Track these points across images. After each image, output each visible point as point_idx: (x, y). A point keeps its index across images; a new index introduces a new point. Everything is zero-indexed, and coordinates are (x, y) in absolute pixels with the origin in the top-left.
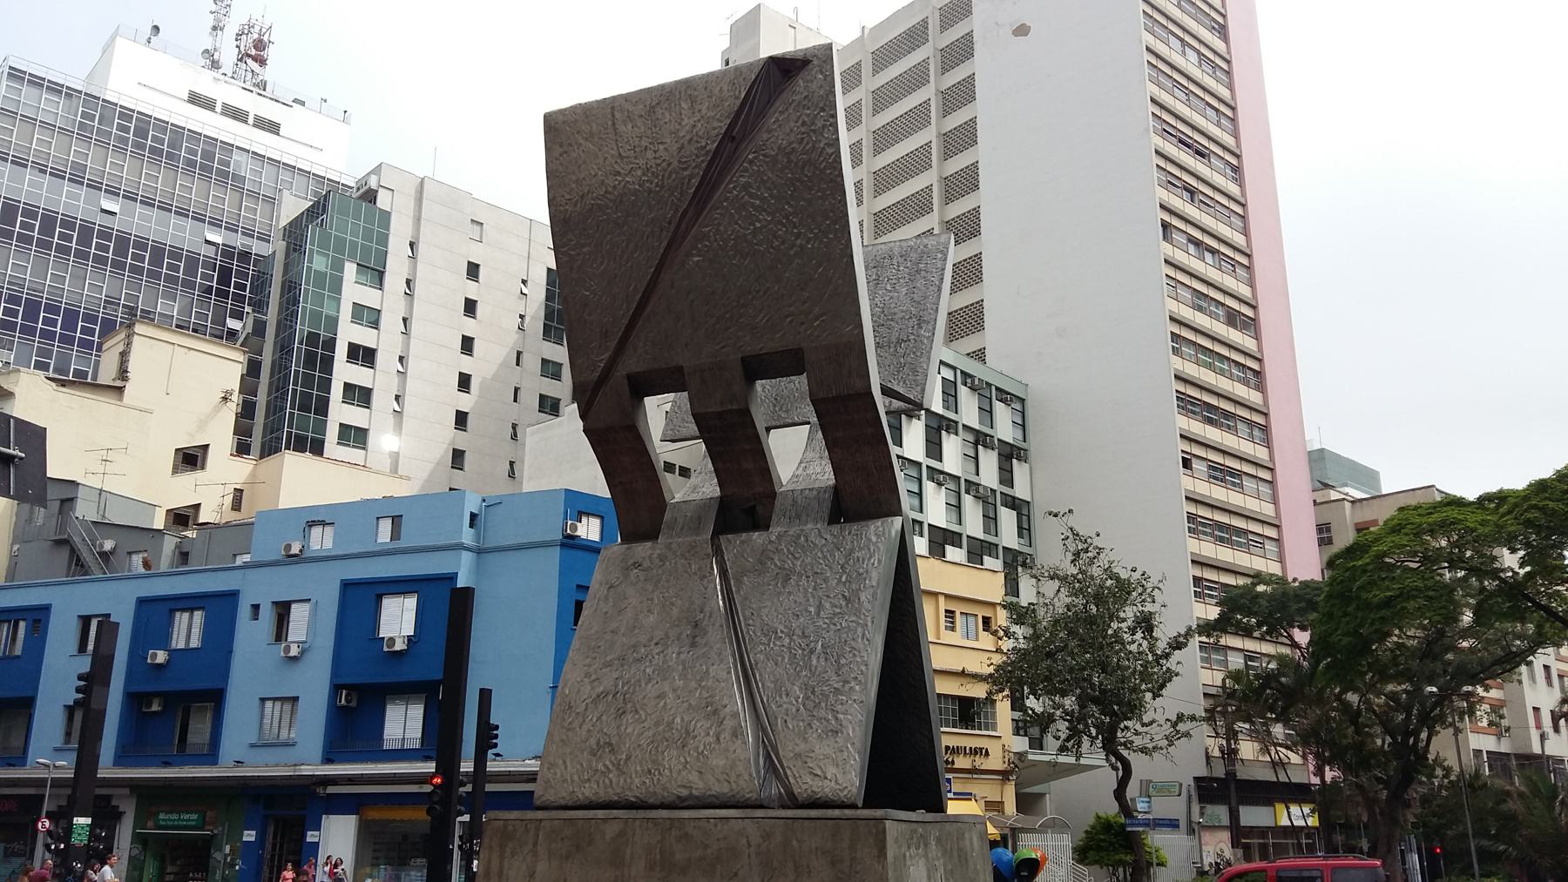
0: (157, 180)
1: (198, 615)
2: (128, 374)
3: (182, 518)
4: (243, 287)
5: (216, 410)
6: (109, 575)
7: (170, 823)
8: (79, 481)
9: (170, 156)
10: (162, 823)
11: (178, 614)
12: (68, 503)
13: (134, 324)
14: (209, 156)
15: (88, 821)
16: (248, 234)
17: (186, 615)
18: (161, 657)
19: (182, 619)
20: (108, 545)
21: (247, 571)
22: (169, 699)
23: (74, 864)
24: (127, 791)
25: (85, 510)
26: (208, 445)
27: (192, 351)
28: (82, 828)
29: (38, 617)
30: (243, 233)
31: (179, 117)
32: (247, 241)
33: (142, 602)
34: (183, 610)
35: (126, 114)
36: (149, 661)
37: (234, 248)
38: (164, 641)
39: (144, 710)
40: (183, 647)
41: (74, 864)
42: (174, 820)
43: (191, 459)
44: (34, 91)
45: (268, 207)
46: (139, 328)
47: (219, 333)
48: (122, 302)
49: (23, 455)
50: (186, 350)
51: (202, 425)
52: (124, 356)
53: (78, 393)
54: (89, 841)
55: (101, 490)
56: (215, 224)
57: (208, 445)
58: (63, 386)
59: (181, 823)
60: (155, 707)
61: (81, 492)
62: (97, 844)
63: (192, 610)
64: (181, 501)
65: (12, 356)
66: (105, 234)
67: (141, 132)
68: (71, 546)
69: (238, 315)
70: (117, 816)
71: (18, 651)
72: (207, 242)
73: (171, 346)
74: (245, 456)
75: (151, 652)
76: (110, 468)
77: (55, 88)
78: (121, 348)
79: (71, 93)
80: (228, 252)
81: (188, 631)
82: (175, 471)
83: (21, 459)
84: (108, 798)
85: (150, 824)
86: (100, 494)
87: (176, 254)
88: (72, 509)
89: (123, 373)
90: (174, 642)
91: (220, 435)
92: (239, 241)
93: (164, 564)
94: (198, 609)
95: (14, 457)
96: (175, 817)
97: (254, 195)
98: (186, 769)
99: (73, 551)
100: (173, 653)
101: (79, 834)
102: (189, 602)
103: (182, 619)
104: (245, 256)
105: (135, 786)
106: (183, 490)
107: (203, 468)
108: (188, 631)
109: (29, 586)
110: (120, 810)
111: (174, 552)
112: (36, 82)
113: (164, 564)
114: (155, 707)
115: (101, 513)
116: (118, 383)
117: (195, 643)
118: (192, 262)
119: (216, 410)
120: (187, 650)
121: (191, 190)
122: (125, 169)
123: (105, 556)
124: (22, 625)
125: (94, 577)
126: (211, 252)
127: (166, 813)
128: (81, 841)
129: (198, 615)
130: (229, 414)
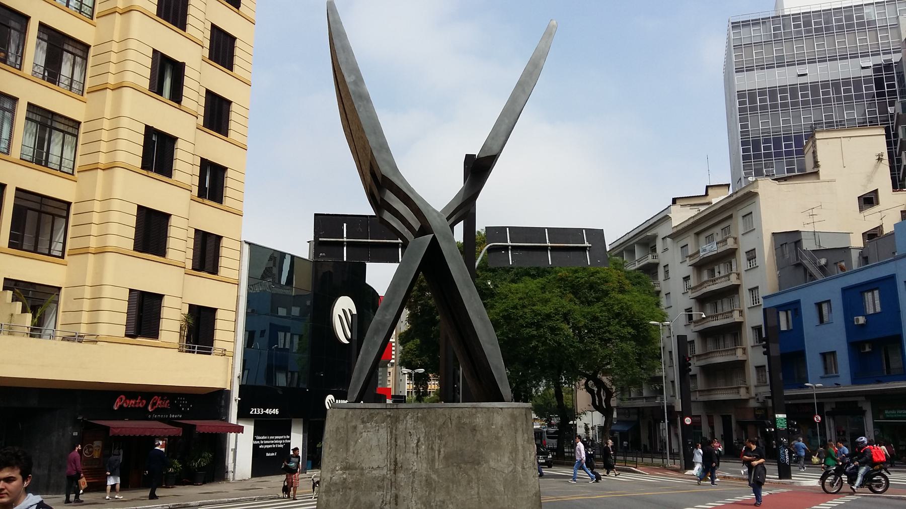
0: (822, 46)
1: (876, 293)
2: (819, 163)
3: (871, 236)
4: (893, 86)
5: (876, 167)
6: (825, 278)
7: (892, 416)
8: (800, 230)
9: (827, 29)
10: (888, 416)
11: (866, 294)
12: (798, 243)
13: (811, 137)
14: (849, 18)
15: (785, 416)
16: (876, 54)
17: (870, 294)
18: (861, 320)
19: (868, 296)
20: (823, 261)
21: (898, 262)
22: (875, 343)
23: (782, 439)
24: (863, 398)
25: (808, 245)
26: (877, 190)
27: (852, 138)
28: (782, 420)
29: (794, 308)
30: (884, 54)
31: (796, 9)
32: (888, 57)
33: (844, 290)
34: (868, 291)
35: (796, 17)
36: (856, 323)
37: (880, 65)
38: (862, 311)
39: (862, 351)
40: (873, 312)
41: (782, 439)
42: (894, 414)
43: (869, 200)
44: (746, 29)
45: (895, 31)
46: (818, 136)
47: (885, 119)
48: (824, 121)
49: (590, 245)
50: (849, 138)
51: (870, 178)
52: (814, 153)
53: (791, 182)
54: (788, 426)
55: (814, 232)
56: (865, 55)
57: (877, 190)
58: (786, 180)
59: (898, 416)
60: (868, 349)
61: (803, 236)
62: (793, 429)
63: (872, 290)
64: (869, 226)
65: (774, 171)
66: (804, 87)
67: (807, 24)
68: (804, 266)
69: (892, 104)
70: (863, 413)
71: (791, 328)
72: (863, 68)
73: (840, 139)
74: (904, 190)
75: (855, 318)
76: (816, 218)
77: (756, 22)
78: (811, 150)
79: (765, 21)
80: (877, 69)
81: (873, 302)
82: (861, 209)
83: (590, 247)
84: (856, 402)
85: (881, 417)
86: (815, 234)
87: (846, 82)
88: (801, 247)
89: (816, 164)
90: (867, 310)
91: (883, 180)
92: (881, 59)
93: (855, 266)
94: (876, 289)
95: (586, 247)
96: (894, 412)
97: (884, 28)
98: (890, 384)
99: (806, 269)
100: (867, 316)
101: (781, 423)
102: (870, 286)
103: (868, 296)
104: (888, 66)
105: (869, 396)
106: (871, 219)
107: (878, 203)
108: (873, 302)
109: (790, 291)
110: (864, 409)
111: (859, 257)
112: (746, 24)
113: (855, 266)
114: (868, 349)
115: (818, 244)
116: (816, 170)
117: (878, 309)
118: (857, 82)
119: (876, 167)
120: (875, 314)
121: (843, 42)
122: (803, 48)
123: (822, 269)
124: (789, 312)
125: (817, 280)
126: (870, 72)
127: (889, 410)
128: (783, 427)
129: (876, 293)
130: (885, 169)
